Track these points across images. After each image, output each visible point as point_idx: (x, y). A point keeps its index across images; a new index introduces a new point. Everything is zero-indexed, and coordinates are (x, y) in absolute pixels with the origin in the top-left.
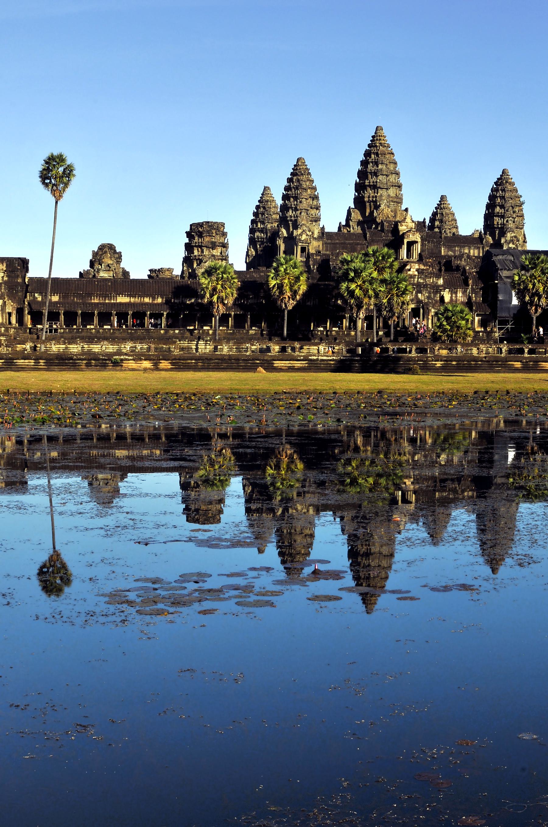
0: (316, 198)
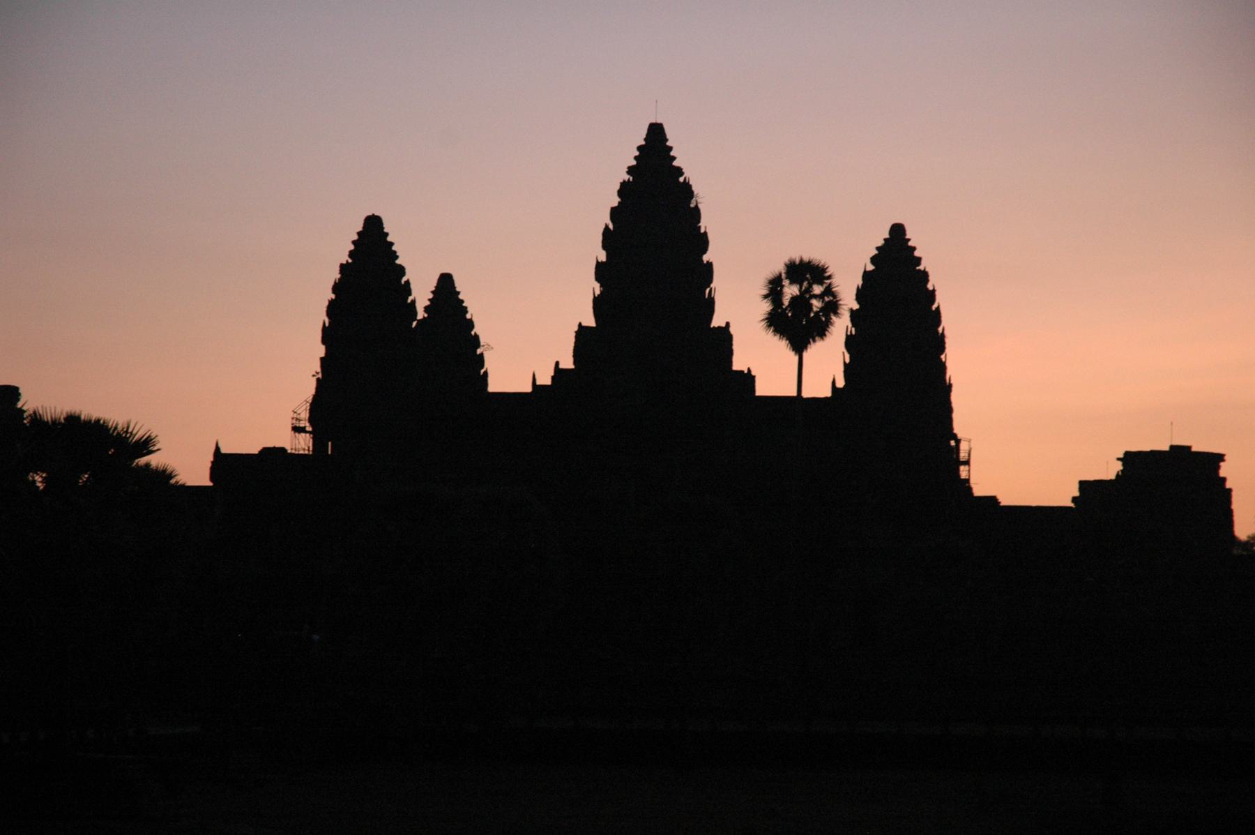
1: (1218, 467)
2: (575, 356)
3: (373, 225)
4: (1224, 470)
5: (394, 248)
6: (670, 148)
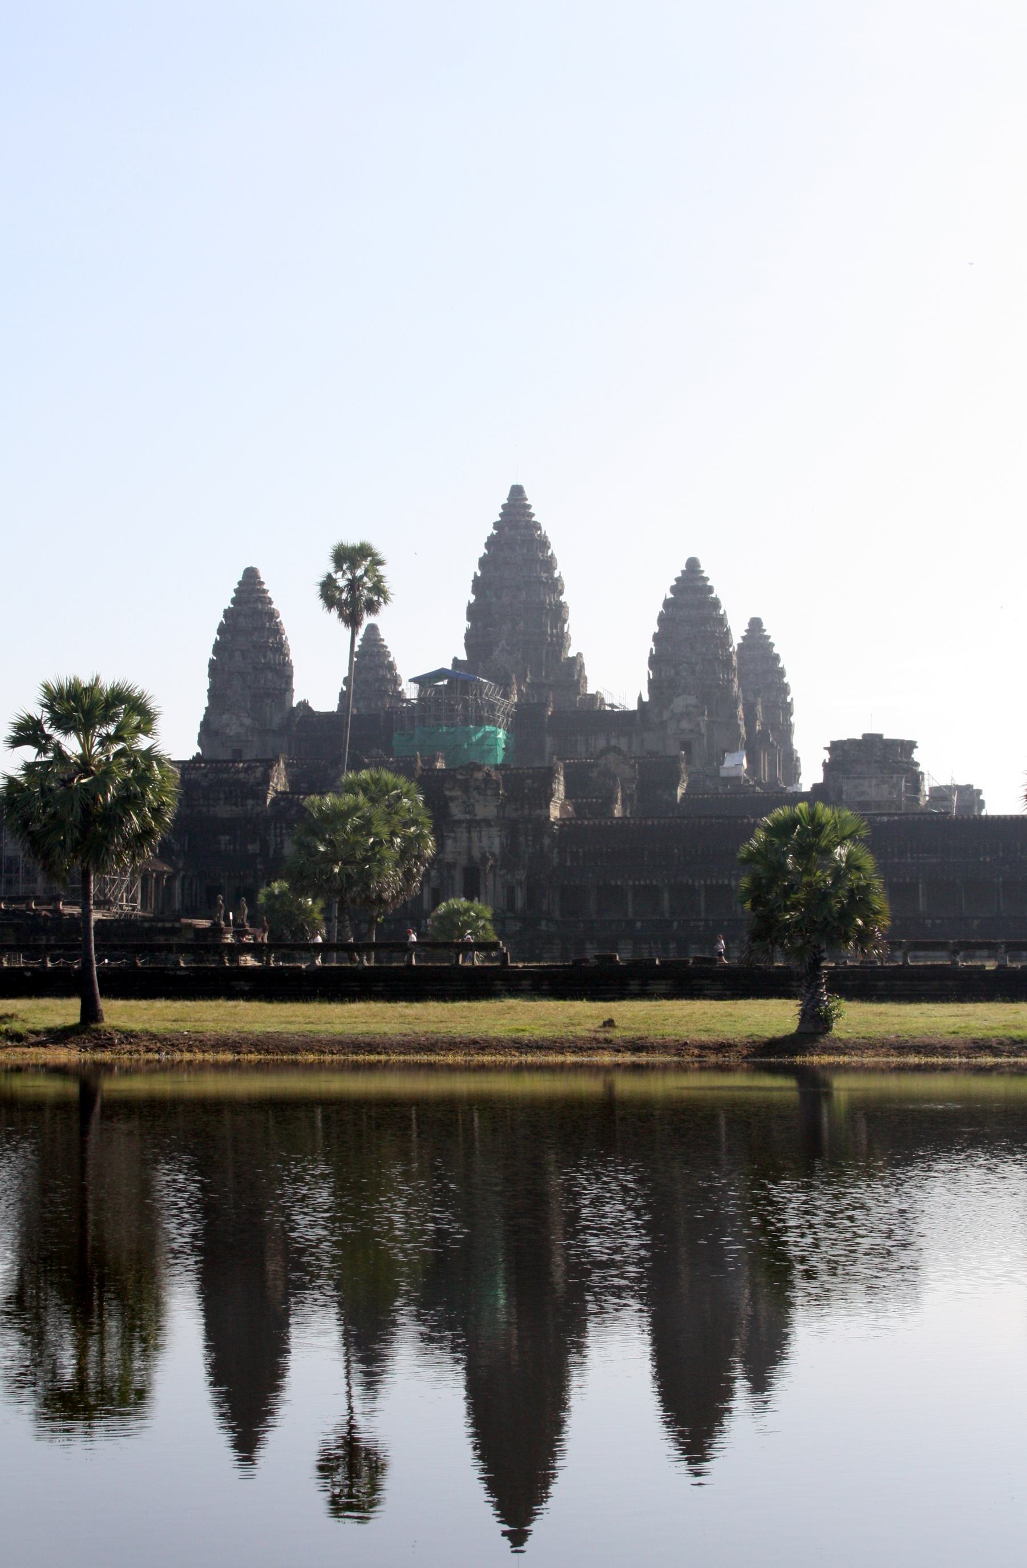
1: (911, 752)
3: (251, 577)
4: (917, 755)
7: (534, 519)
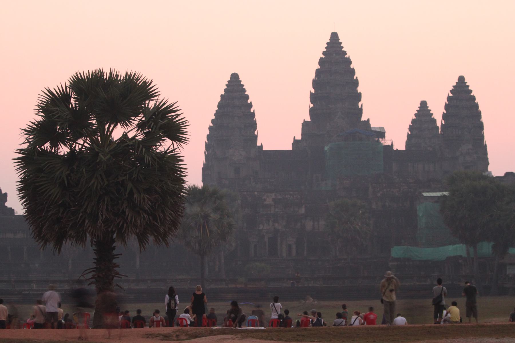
0: (253, 115)
2: (302, 135)
5: (244, 87)
6: (341, 43)
7: (343, 50)
